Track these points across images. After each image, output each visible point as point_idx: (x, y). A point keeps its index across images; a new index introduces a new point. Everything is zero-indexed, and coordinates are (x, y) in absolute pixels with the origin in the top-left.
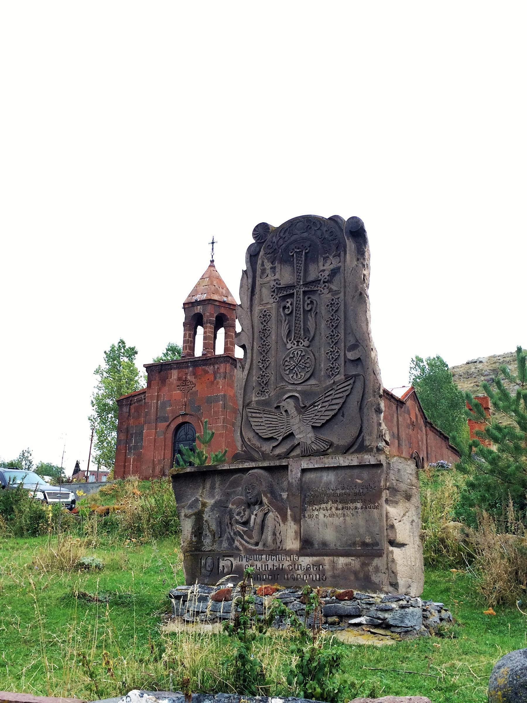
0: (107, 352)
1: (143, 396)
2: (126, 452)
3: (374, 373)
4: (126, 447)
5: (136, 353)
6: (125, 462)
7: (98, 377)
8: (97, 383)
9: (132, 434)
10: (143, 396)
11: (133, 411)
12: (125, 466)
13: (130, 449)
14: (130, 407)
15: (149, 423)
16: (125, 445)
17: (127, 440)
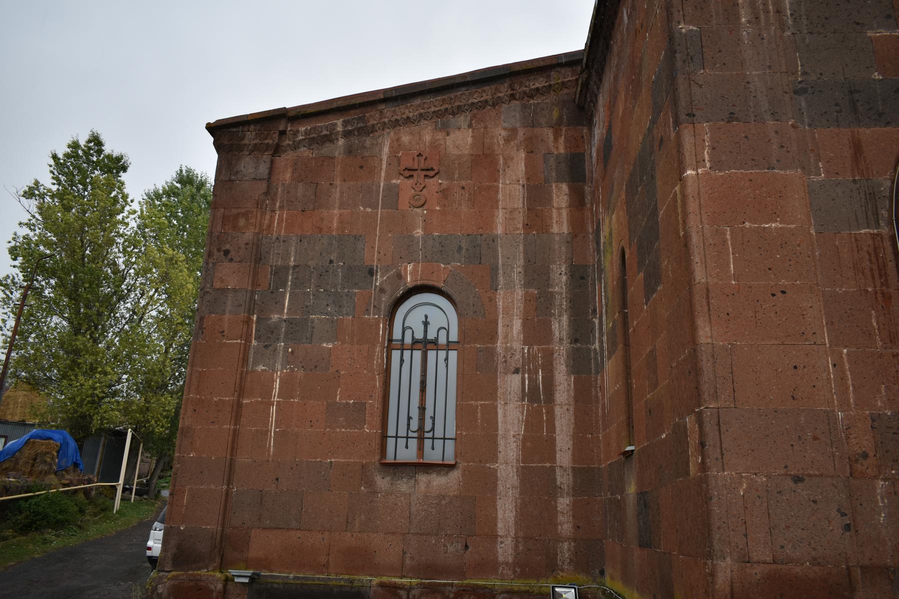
0: (60, 156)
1: (339, 122)
2: (247, 346)
3: (421, 293)
4: (248, 322)
5: (124, 169)
6: (241, 391)
7: (33, 204)
8: (25, 218)
9: (280, 273)
10: (339, 122)
11: (286, 176)
12: (238, 407)
13: (269, 334)
14: (272, 162)
15: (732, 118)
16: (243, 315)
17: (253, 293)
